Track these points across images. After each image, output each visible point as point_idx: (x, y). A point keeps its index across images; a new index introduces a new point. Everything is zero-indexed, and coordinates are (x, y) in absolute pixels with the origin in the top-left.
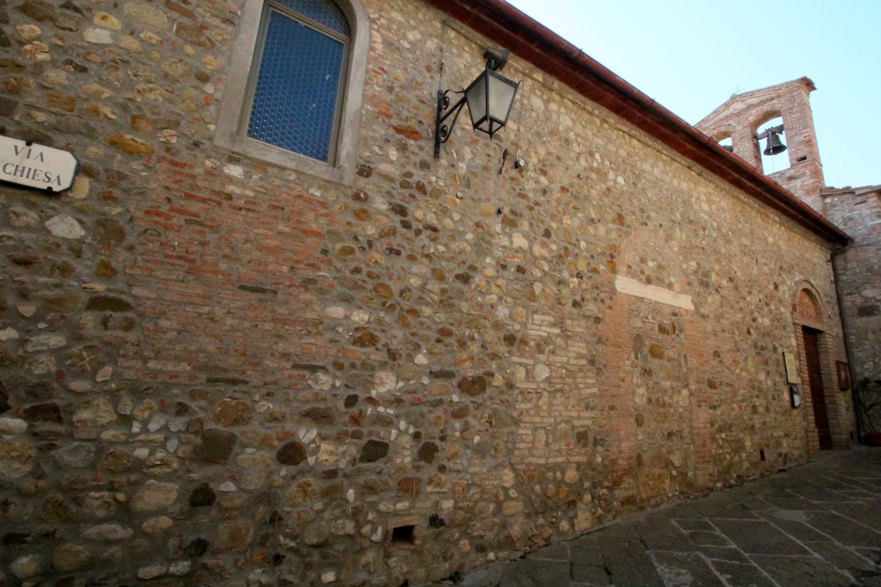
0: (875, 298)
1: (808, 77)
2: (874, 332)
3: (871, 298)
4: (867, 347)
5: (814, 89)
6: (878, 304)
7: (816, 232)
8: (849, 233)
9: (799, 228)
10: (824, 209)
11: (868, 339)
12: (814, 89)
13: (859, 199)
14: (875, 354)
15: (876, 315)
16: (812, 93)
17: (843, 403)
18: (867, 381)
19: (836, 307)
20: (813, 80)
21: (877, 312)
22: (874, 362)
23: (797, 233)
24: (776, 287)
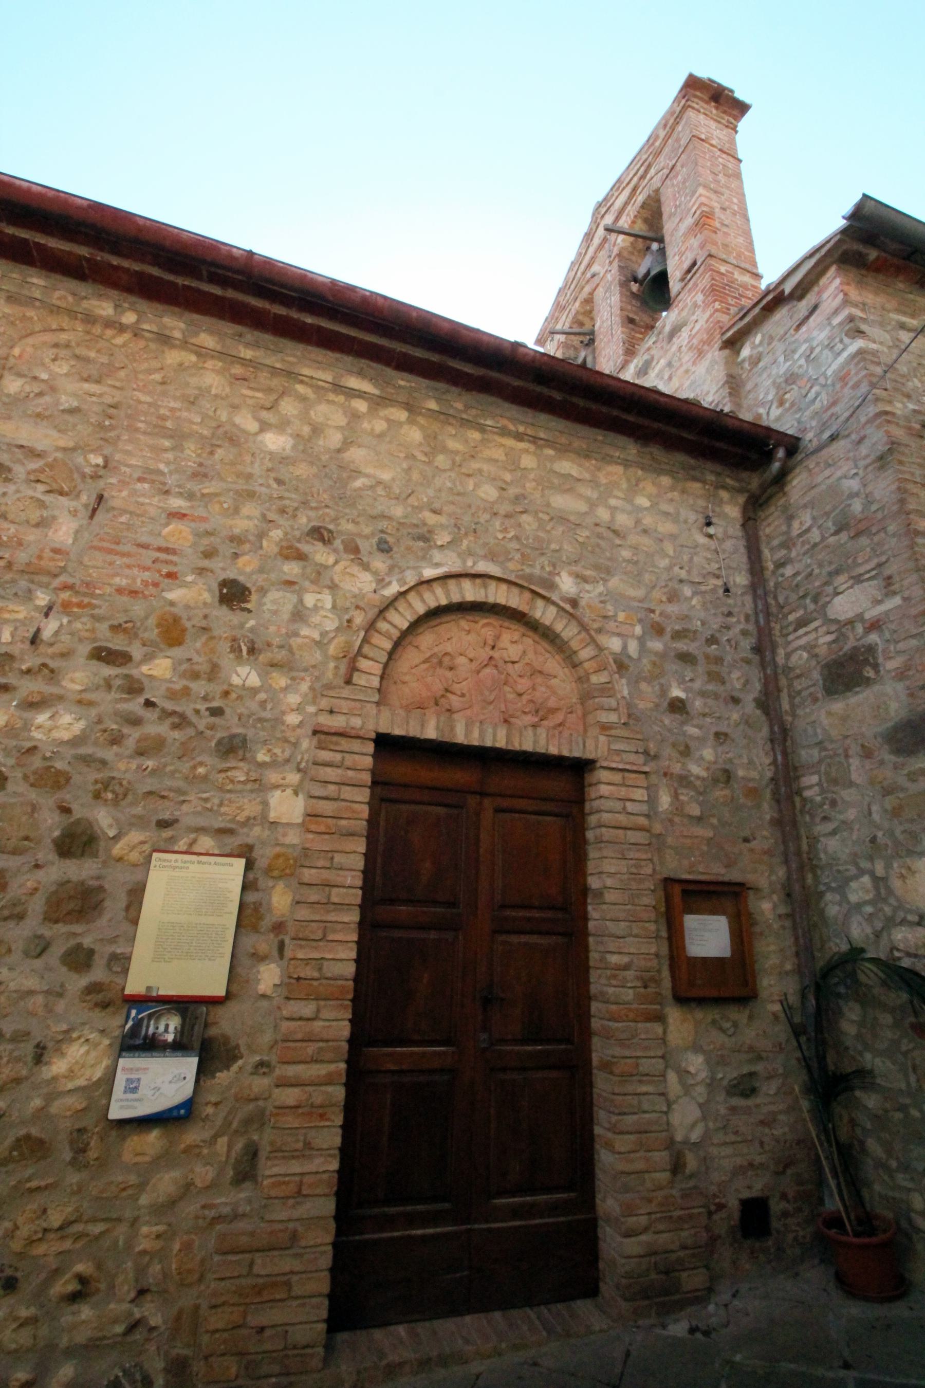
0: (860, 617)
1: (703, 73)
2: (867, 754)
3: (850, 622)
4: (851, 814)
5: (742, 108)
6: (873, 638)
7: (671, 444)
8: (788, 426)
9: (547, 425)
10: (734, 384)
11: (851, 784)
12: (742, 108)
13: (803, 306)
14: (873, 840)
15: (868, 682)
16: (744, 124)
17: (696, 1063)
18: (856, 953)
19: (743, 679)
20: (725, 82)
21: (869, 673)
22: (872, 874)
23: (504, 432)
24: (233, 594)
